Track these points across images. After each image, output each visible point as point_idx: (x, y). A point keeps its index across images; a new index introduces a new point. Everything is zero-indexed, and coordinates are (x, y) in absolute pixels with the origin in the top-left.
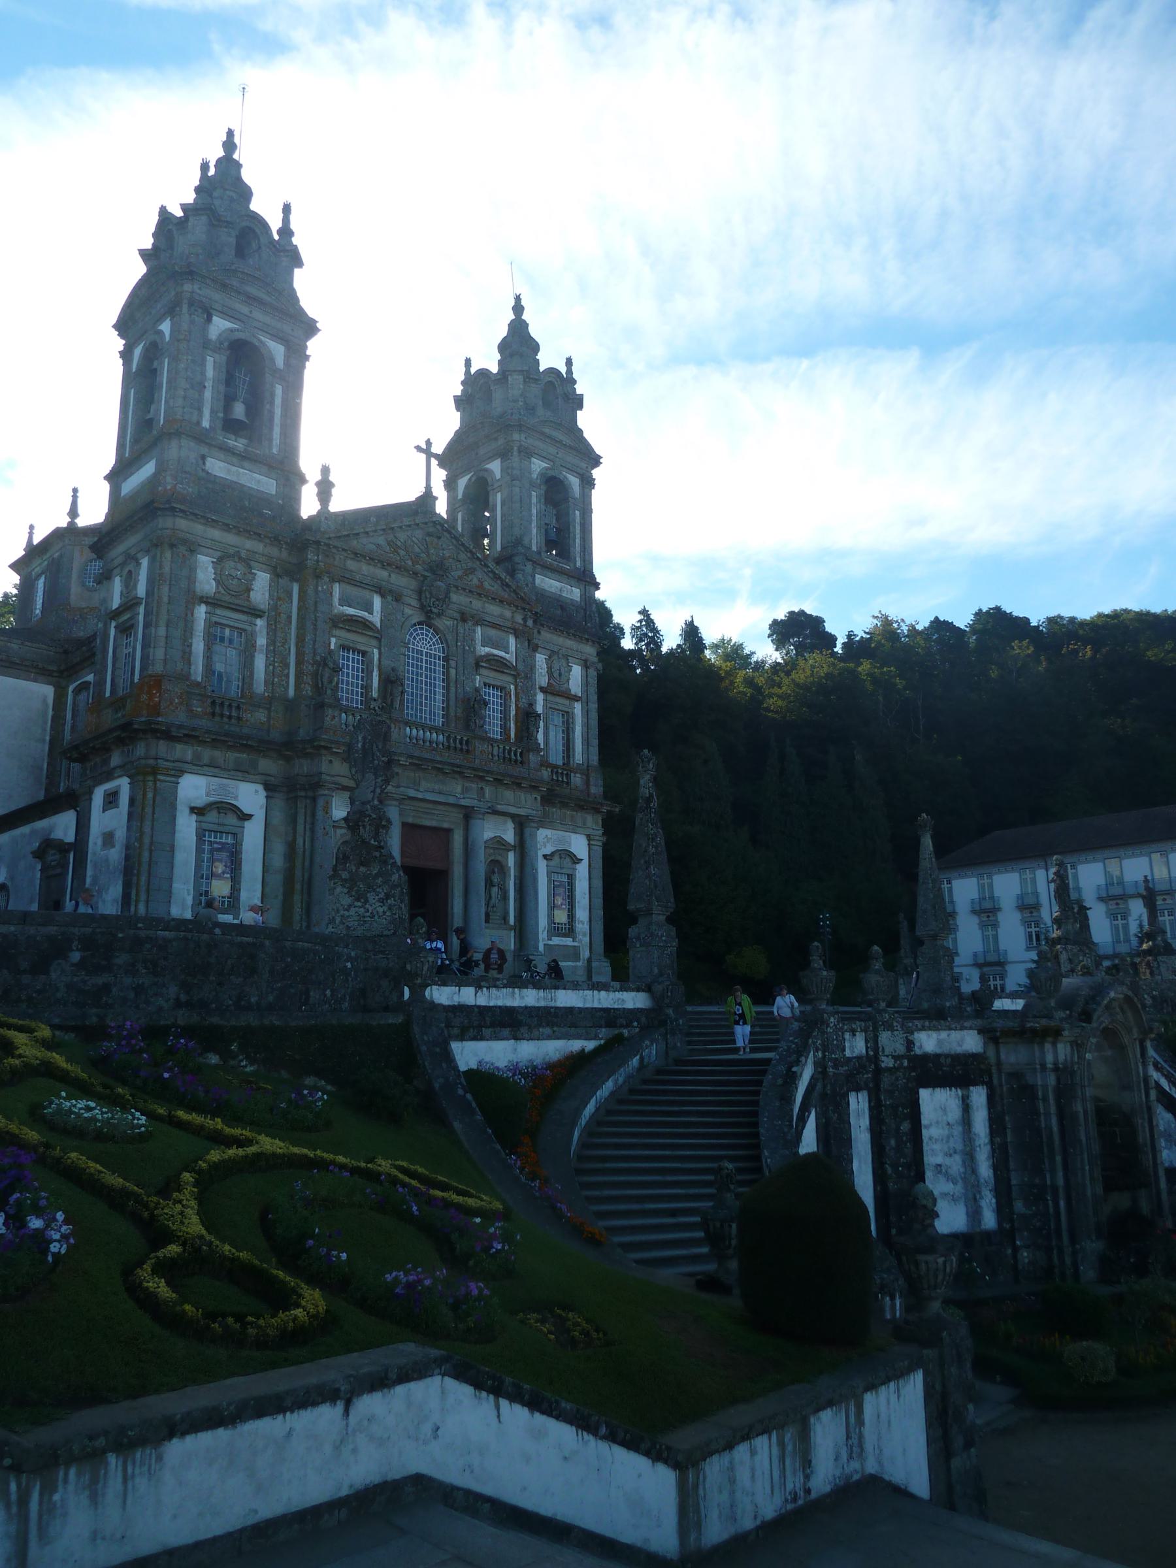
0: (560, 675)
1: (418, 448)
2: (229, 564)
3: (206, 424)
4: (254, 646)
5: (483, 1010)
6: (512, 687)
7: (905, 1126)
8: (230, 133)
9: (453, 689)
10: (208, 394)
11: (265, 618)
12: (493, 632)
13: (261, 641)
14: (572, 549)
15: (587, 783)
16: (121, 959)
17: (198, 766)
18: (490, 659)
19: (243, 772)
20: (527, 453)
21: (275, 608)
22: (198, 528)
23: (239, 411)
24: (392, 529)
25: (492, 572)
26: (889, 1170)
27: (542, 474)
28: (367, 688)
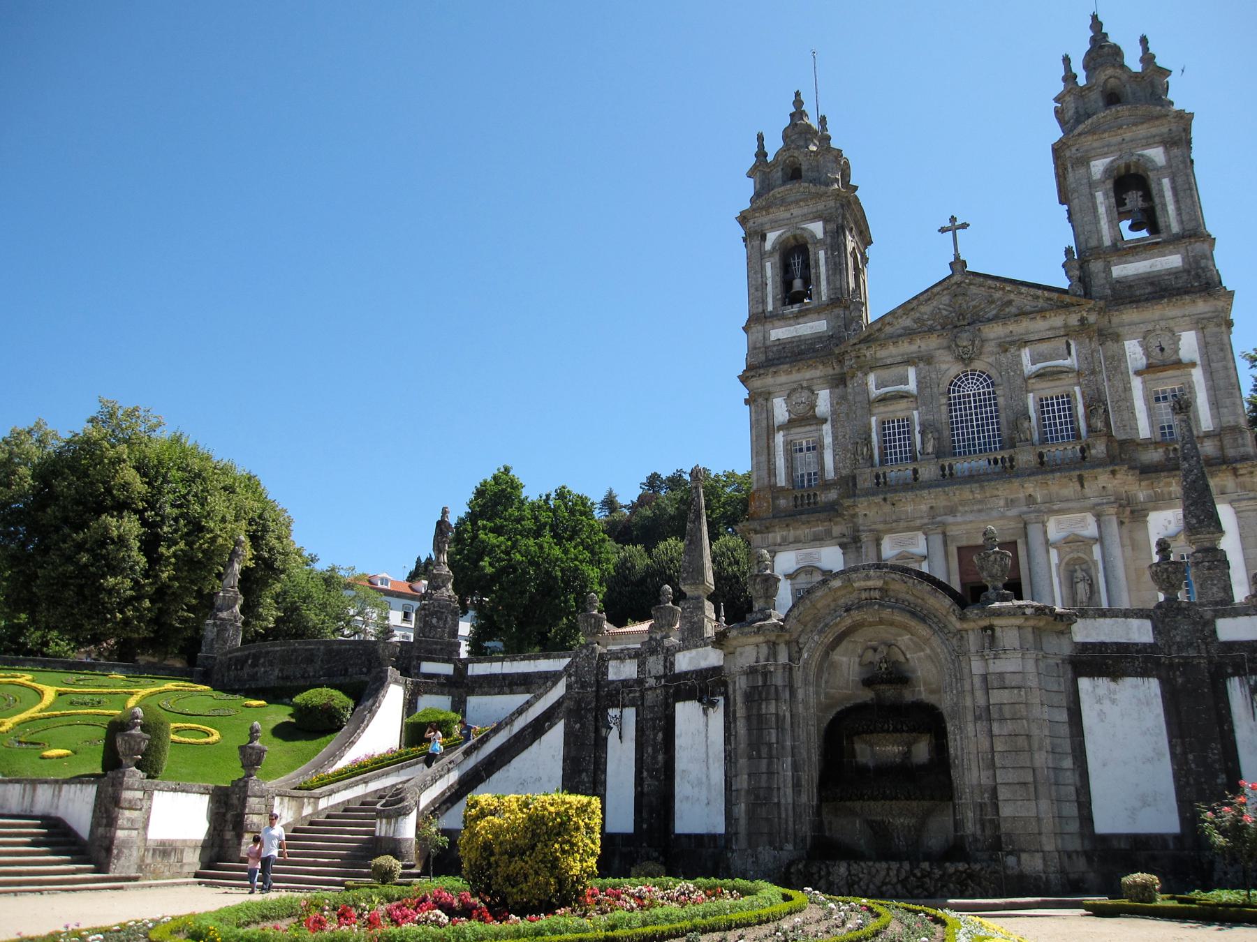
0: (1162, 350)
1: (943, 230)
2: (796, 398)
3: (770, 308)
4: (822, 447)
5: (505, 676)
6: (1077, 389)
7: (660, 735)
8: (797, 94)
9: (1003, 416)
10: (769, 288)
11: (829, 422)
12: (1044, 347)
13: (828, 440)
14: (1161, 222)
15: (1222, 448)
16: (262, 661)
17: (785, 544)
18: (1040, 375)
19: (819, 540)
20: (1084, 161)
21: (834, 412)
22: (769, 380)
23: (798, 284)
24: (913, 309)
25: (1028, 294)
26: (645, 774)
27: (1108, 171)
28: (912, 445)
